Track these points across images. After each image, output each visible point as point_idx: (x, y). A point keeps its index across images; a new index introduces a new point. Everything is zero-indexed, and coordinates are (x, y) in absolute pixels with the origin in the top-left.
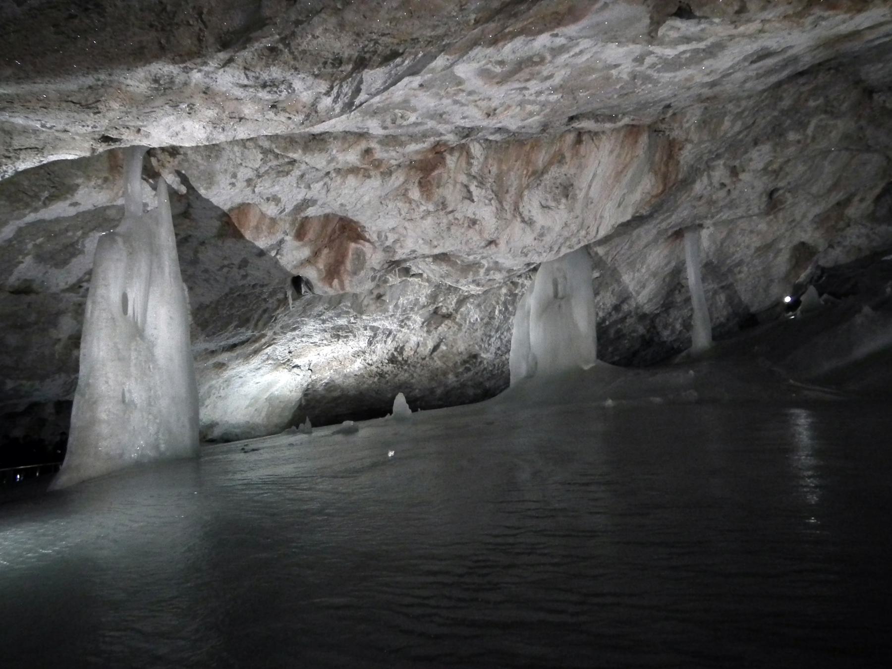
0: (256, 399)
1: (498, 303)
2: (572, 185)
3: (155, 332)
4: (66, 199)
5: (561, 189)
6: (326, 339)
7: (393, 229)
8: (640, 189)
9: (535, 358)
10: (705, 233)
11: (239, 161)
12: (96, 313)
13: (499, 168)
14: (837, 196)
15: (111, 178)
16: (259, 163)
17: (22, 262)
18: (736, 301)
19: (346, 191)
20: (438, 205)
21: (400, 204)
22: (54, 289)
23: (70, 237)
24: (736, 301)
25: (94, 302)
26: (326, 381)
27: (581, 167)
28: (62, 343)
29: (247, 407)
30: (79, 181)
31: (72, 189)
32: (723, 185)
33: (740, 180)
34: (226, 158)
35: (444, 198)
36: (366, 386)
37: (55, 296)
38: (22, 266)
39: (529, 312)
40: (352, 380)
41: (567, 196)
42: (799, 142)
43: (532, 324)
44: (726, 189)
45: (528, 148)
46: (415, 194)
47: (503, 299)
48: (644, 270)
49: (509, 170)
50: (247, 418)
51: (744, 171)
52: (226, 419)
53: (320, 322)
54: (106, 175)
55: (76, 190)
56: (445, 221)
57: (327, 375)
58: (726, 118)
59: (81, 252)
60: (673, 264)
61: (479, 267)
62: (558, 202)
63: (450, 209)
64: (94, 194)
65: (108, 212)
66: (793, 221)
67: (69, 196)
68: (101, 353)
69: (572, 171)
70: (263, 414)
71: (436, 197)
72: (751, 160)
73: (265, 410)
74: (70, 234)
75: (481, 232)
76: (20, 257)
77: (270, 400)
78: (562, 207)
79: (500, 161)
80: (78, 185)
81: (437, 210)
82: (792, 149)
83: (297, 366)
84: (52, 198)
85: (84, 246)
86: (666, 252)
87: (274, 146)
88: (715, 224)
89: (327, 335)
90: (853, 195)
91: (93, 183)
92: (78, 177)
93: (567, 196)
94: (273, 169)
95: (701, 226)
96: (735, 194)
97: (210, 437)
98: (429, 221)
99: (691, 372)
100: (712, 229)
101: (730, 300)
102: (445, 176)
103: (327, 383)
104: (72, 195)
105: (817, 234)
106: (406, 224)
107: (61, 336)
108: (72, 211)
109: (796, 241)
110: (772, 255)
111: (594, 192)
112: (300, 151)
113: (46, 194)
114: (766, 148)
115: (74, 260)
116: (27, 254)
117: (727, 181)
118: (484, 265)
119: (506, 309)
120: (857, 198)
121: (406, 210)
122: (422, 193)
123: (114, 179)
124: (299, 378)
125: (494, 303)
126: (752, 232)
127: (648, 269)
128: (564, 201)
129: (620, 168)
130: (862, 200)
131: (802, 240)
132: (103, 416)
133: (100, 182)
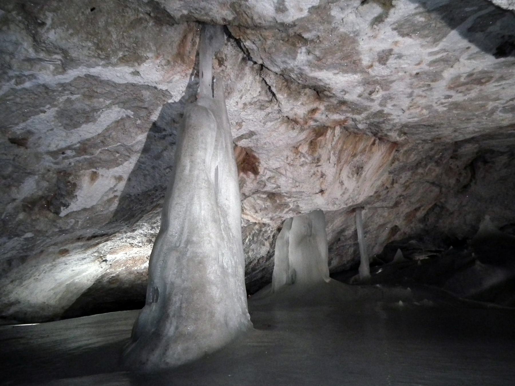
0: (60, 284)
1: (250, 234)
2: (362, 168)
3: (227, 202)
4: (133, 66)
5: (356, 168)
6: (142, 242)
7: (276, 169)
8: (382, 178)
9: (295, 272)
10: (363, 212)
11: (249, 88)
12: (196, 172)
13: (342, 147)
14: (418, 206)
15: (172, 63)
16: (258, 93)
17: (45, 112)
18: (357, 252)
19: (275, 134)
20: (314, 159)
21: (290, 154)
22: (42, 149)
23: (100, 102)
24: (357, 252)
25: (192, 162)
26: (114, 275)
27: (370, 158)
28: (15, 204)
29: (50, 291)
30: (150, 55)
31: (139, 59)
32: (387, 188)
33: (394, 187)
34: (245, 81)
35: (320, 156)
36: (140, 282)
37: (38, 157)
38: (42, 115)
39: (287, 242)
40: (132, 276)
41: (358, 174)
42: (422, 174)
43: (290, 249)
44: (387, 190)
45: (358, 139)
46: (304, 149)
47: (253, 232)
48: (330, 228)
49: (346, 149)
50: (45, 300)
51: (397, 183)
52: (29, 299)
53: (150, 228)
54: (169, 59)
55: (144, 61)
56: (312, 171)
57: (119, 270)
58: (414, 153)
59: (94, 120)
60: (344, 227)
61: (286, 207)
62: (353, 175)
63: (319, 164)
64: (154, 70)
65: (144, 92)
66: (398, 214)
67: (136, 64)
68: (203, 212)
69: (365, 160)
70: (58, 297)
71: (316, 155)
72: (401, 178)
73: (61, 294)
74: (101, 100)
75: (322, 183)
76: (48, 106)
77: (68, 286)
78: (354, 179)
79: (344, 143)
80: (147, 58)
81: (313, 163)
82: (418, 177)
83: (106, 261)
84: (124, 60)
85: (99, 116)
86: (343, 220)
87: (274, 85)
88: (369, 209)
89: (145, 239)
90: (422, 206)
91: (158, 61)
92: (151, 51)
93: (358, 174)
94: (260, 102)
95: (363, 208)
96: (389, 194)
97: (4, 314)
98: (306, 168)
99: (409, 289)
100: (367, 211)
101: (355, 251)
102: (323, 143)
103: (113, 277)
104: (139, 65)
105: (404, 223)
106: (288, 167)
107: (18, 196)
108: (131, 79)
109: (395, 224)
110: (382, 230)
111: (367, 176)
112: (286, 95)
113: (120, 54)
114: (409, 174)
115: (84, 126)
116: (55, 106)
117: (389, 186)
118: (290, 206)
119: (253, 239)
120: (422, 208)
121: (292, 158)
122: (309, 148)
123: (174, 66)
124: (101, 270)
125: (248, 234)
126: (381, 216)
127: (333, 227)
128: (355, 175)
129: (381, 165)
130: (424, 209)
131: (397, 225)
132: (212, 277)
133: (164, 62)
